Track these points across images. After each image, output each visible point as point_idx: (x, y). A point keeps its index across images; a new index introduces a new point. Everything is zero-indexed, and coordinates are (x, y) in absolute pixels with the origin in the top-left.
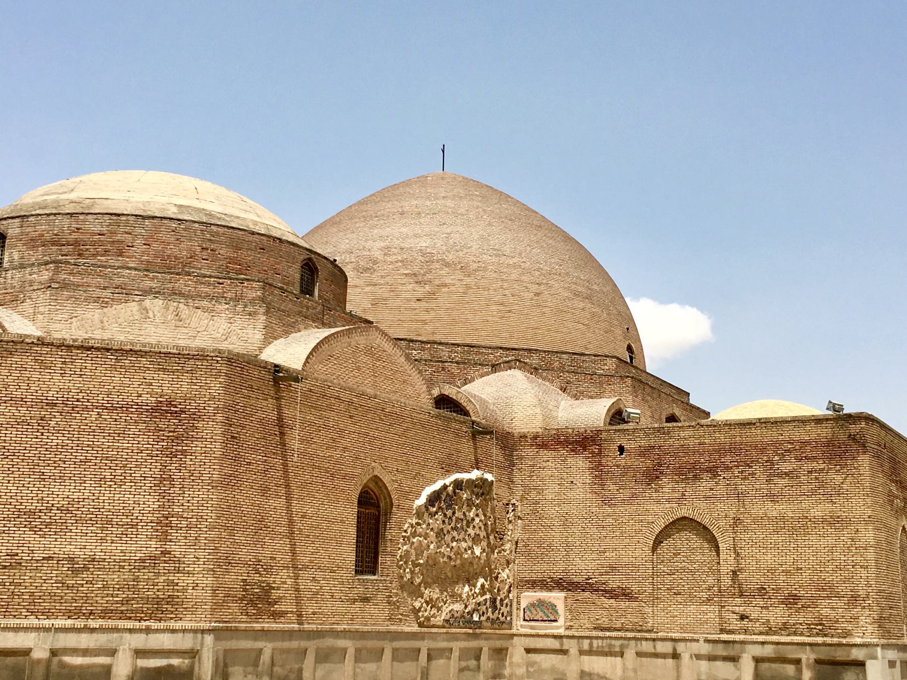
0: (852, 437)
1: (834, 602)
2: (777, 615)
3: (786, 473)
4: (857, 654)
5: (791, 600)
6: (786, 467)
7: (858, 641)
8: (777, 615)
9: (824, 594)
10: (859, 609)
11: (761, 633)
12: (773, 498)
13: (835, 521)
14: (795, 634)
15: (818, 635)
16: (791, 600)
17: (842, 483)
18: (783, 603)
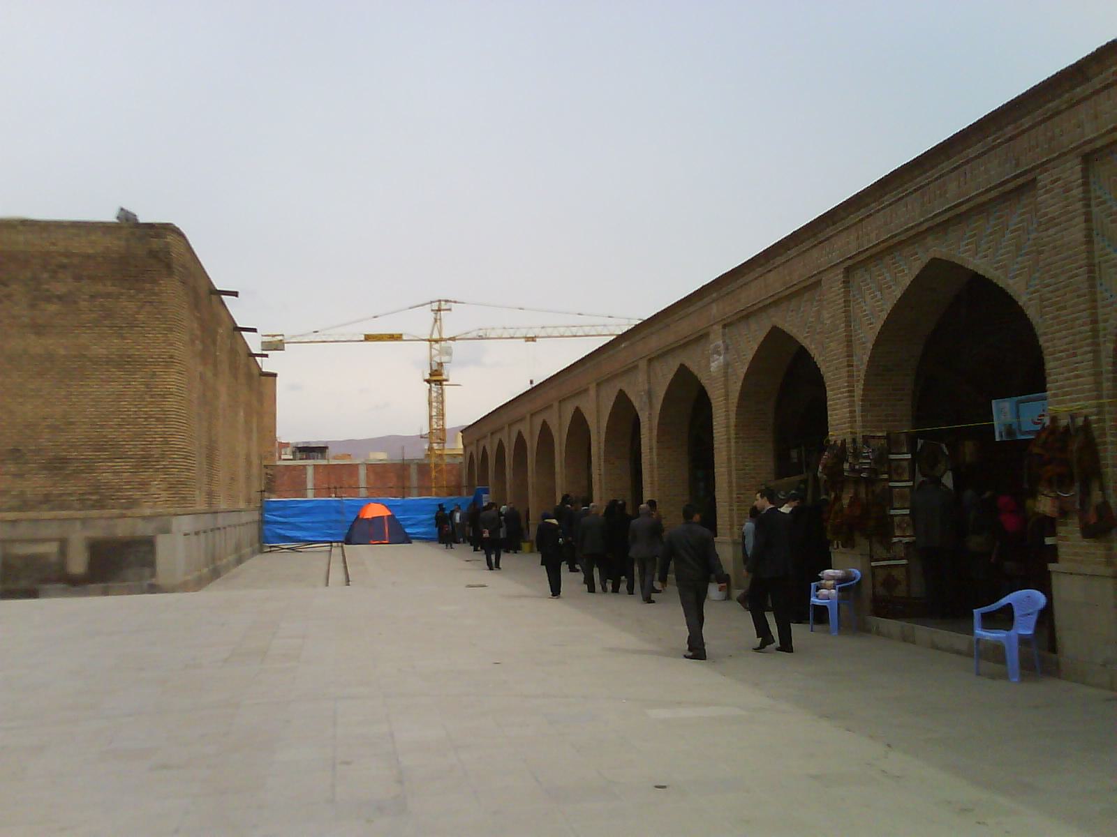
0: (153, 254)
1: (119, 465)
2: (36, 484)
3: (60, 298)
4: (144, 529)
5: (57, 465)
6: (60, 288)
7: (148, 512)
8: (36, 484)
9: (104, 455)
10: (150, 472)
11: (11, 509)
12: (39, 329)
13: (124, 362)
14: (62, 507)
15: (93, 507)
16: (57, 465)
17: (138, 313)
18: (45, 468)
